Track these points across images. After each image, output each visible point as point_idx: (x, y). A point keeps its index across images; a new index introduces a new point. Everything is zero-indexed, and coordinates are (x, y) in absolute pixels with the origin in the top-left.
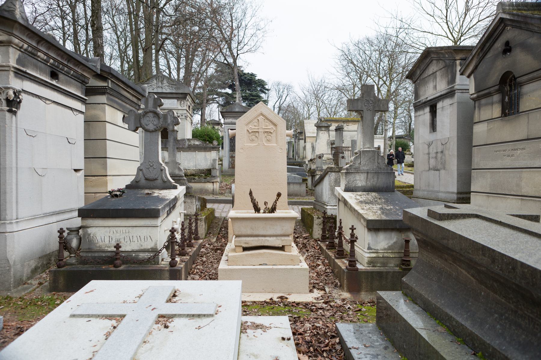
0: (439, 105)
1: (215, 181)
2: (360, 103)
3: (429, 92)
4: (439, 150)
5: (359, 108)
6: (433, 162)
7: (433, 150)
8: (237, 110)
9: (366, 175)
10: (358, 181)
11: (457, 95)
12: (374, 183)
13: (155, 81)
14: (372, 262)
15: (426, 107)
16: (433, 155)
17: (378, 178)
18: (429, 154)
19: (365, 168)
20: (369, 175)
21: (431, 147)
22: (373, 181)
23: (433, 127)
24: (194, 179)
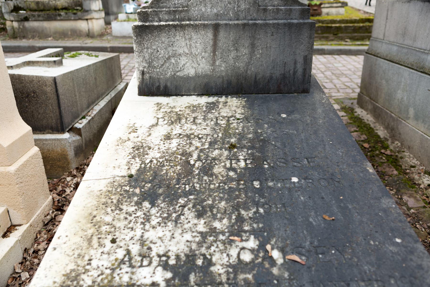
1: (88, 17)
9: (210, 35)
10: (183, 61)
12: (241, 65)
17: (253, 46)
20: (222, 34)
24: (60, 15)
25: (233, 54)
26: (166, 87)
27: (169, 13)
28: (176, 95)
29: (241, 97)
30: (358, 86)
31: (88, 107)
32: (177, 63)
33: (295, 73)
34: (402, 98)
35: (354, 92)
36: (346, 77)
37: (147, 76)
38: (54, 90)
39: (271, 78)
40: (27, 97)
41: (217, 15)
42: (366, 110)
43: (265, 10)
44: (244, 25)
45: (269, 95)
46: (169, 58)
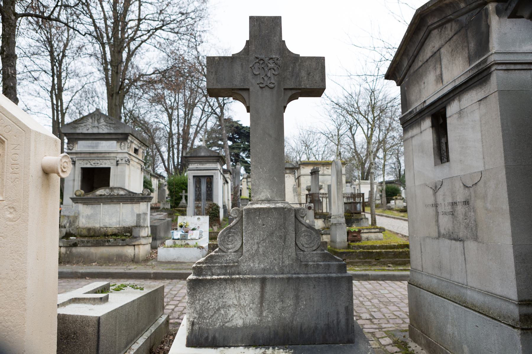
0: (452, 110)
1: (136, 243)
2: (237, 68)
3: (429, 91)
4: (460, 198)
5: (237, 83)
6: (445, 222)
7: (444, 199)
8: (203, 154)
10: (232, 312)
11: (496, 78)
12: (286, 315)
13: (90, 120)
15: (423, 119)
16: (444, 207)
17: (297, 297)
18: (436, 205)
19: (256, 265)
20: (269, 287)
21: (440, 193)
22: (282, 310)
23: (442, 153)
24: (108, 241)
25: (279, 305)
26: (214, 338)
27: (221, 268)
28: (224, 346)
29: (287, 349)
30: (407, 315)
31: (126, 347)
32: (226, 314)
33: (338, 323)
34: (453, 334)
35: (404, 322)
36: (394, 305)
37: (196, 327)
38: (96, 331)
39: (316, 328)
40: (66, 338)
41: (264, 270)
42: (420, 344)
43: (307, 265)
44: (289, 279)
45: (315, 345)
46: (219, 309)
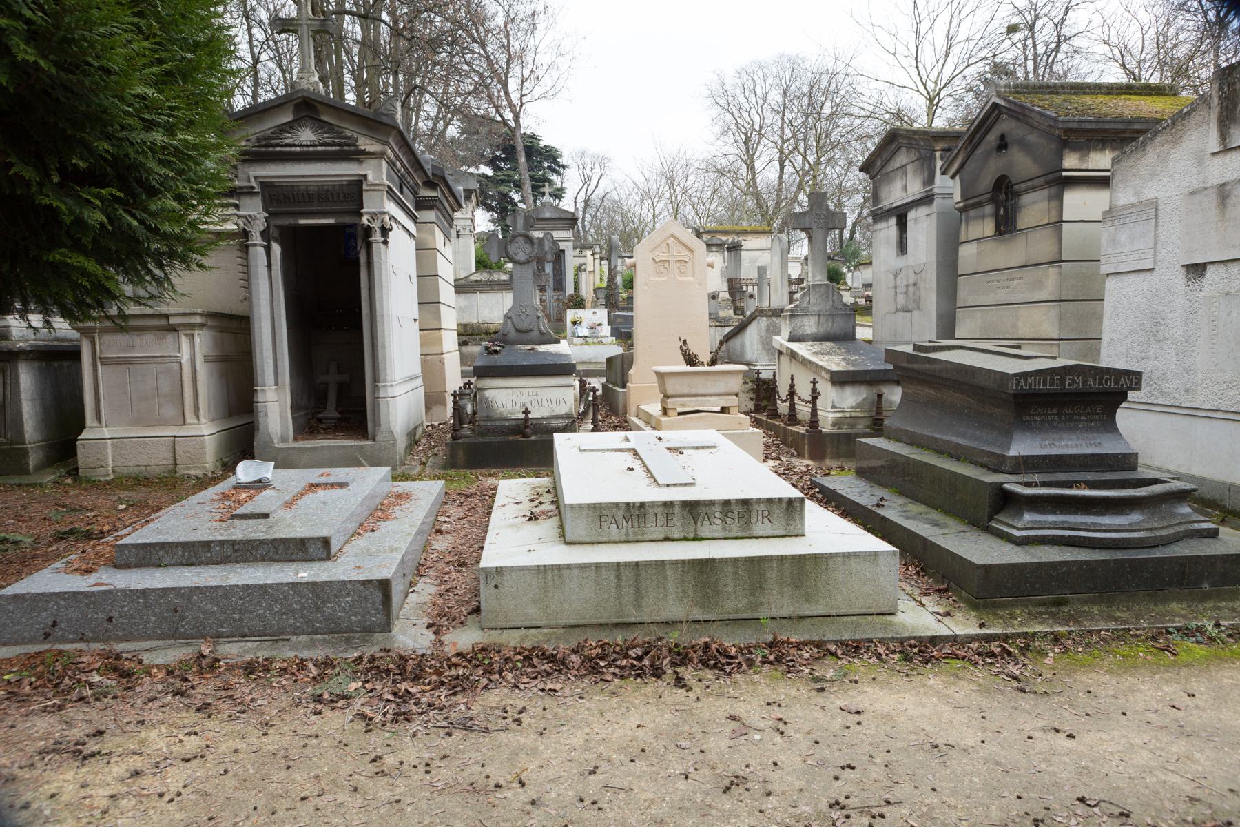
0: (911, 215)
3: (895, 195)
4: (911, 282)
5: (807, 226)
6: (901, 300)
7: (901, 282)
8: (548, 215)
11: (937, 202)
14: (837, 423)
15: (890, 216)
16: (901, 289)
18: (895, 287)
19: (816, 309)
21: (899, 278)
22: (827, 327)
23: (902, 247)
